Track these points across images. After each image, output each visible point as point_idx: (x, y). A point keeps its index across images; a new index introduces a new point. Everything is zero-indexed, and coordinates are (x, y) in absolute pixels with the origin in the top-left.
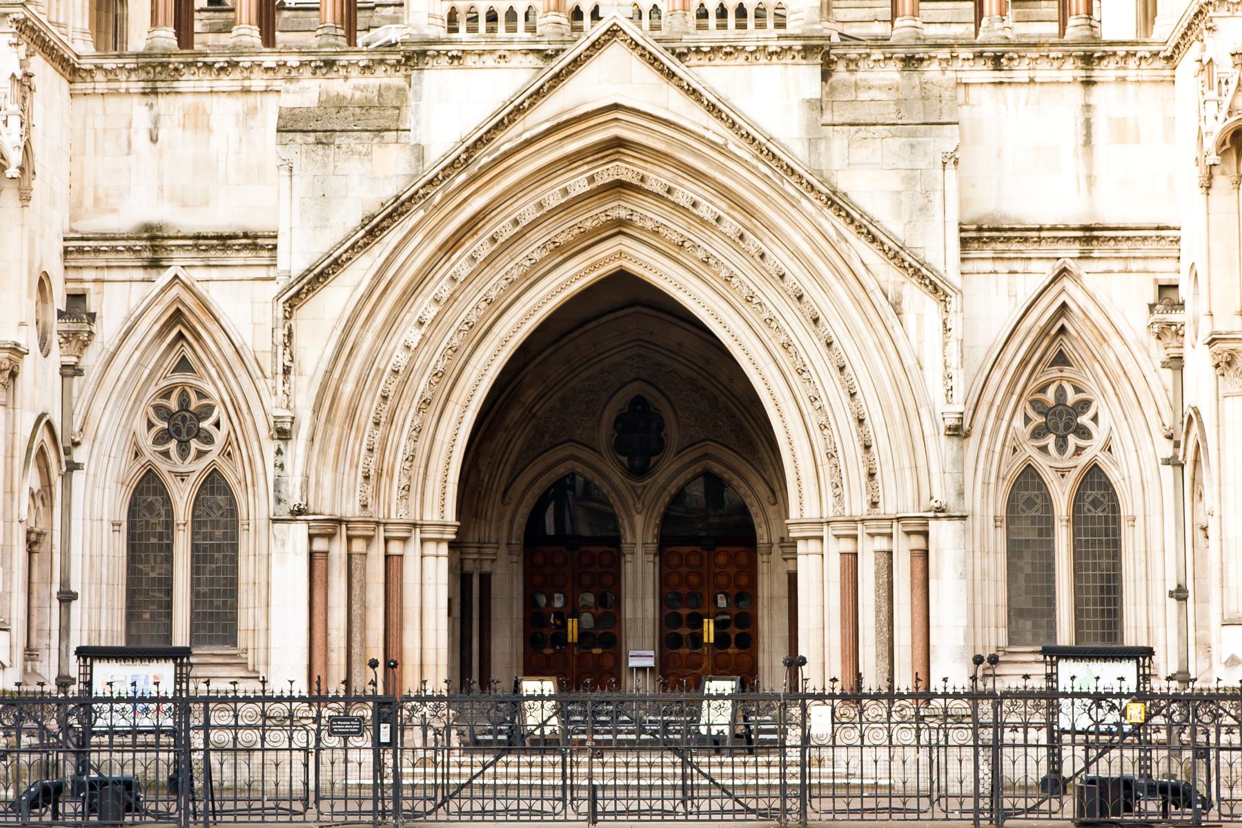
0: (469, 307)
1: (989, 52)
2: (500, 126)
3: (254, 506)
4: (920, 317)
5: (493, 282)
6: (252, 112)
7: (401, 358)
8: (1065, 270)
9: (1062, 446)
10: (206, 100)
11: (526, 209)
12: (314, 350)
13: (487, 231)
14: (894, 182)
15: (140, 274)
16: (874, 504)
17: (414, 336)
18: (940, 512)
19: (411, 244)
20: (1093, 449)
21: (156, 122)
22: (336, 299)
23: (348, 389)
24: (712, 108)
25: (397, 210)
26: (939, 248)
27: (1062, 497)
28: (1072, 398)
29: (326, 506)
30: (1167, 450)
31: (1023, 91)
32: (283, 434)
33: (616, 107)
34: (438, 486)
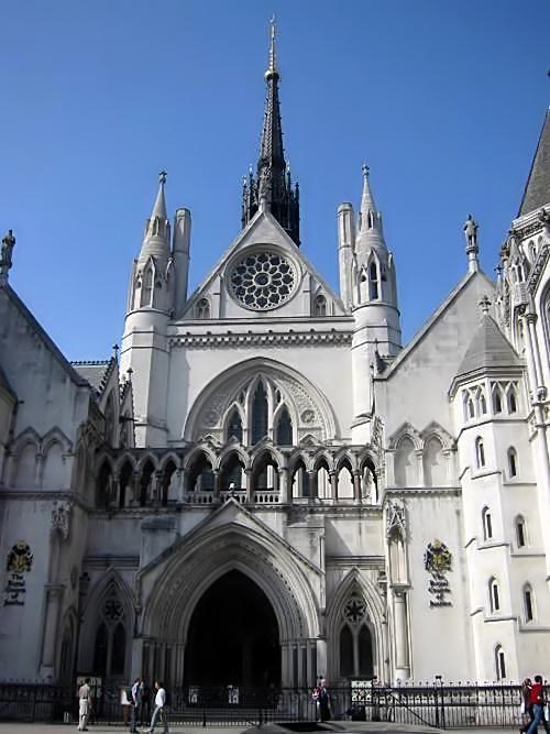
2: (201, 528)
3: (130, 633)
4: (314, 581)
6: (136, 525)
8: (354, 570)
9: (355, 618)
12: (147, 591)
14: (307, 544)
17: (175, 586)
18: (321, 638)
19: (177, 561)
20: (364, 620)
22: (153, 576)
24: (257, 524)
26: (318, 560)
27: (355, 633)
28: (358, 605)
29: (148, 632)
30: (383, 619)
32: (138, 613)
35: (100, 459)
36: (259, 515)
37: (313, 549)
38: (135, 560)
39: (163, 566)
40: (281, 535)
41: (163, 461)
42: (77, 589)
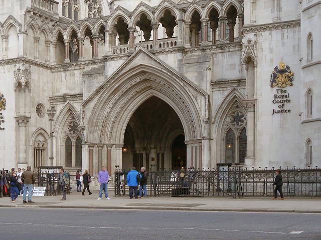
0: (121, 104)
1: (219, 46)
5: (125, 100)
7: (106, 114)
10: (74, 71)
11: (129, 86)
13: (121, 91)
14: (196, 74)
15: (63, 103)
16: (195, 137)
17: (109, 111)
21: (66, 75)
22: (92, 104)
23: (95, 120)
25: (101, 88)
26: (206, 87)
31: (228, 53)
33: (141, 65)
34: (119, 137)
35: (55, 31)
36: (161, 57)
37: (201, 77)
38: (80, 95)
39: (97, 98)
40: (177, 70)
41: (96, 27)
42: (47, 117)
